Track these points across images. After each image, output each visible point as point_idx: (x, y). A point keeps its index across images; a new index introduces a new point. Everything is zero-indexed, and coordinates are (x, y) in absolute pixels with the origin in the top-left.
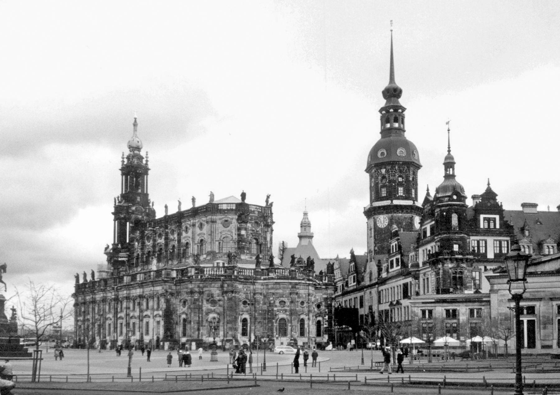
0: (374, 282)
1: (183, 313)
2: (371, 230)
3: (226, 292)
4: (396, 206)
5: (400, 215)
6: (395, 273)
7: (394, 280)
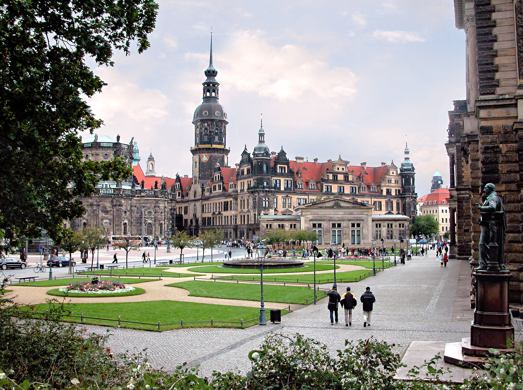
0: (197, 198)
3: (115, 205)
4: (214, 149)
6: (217, 194)
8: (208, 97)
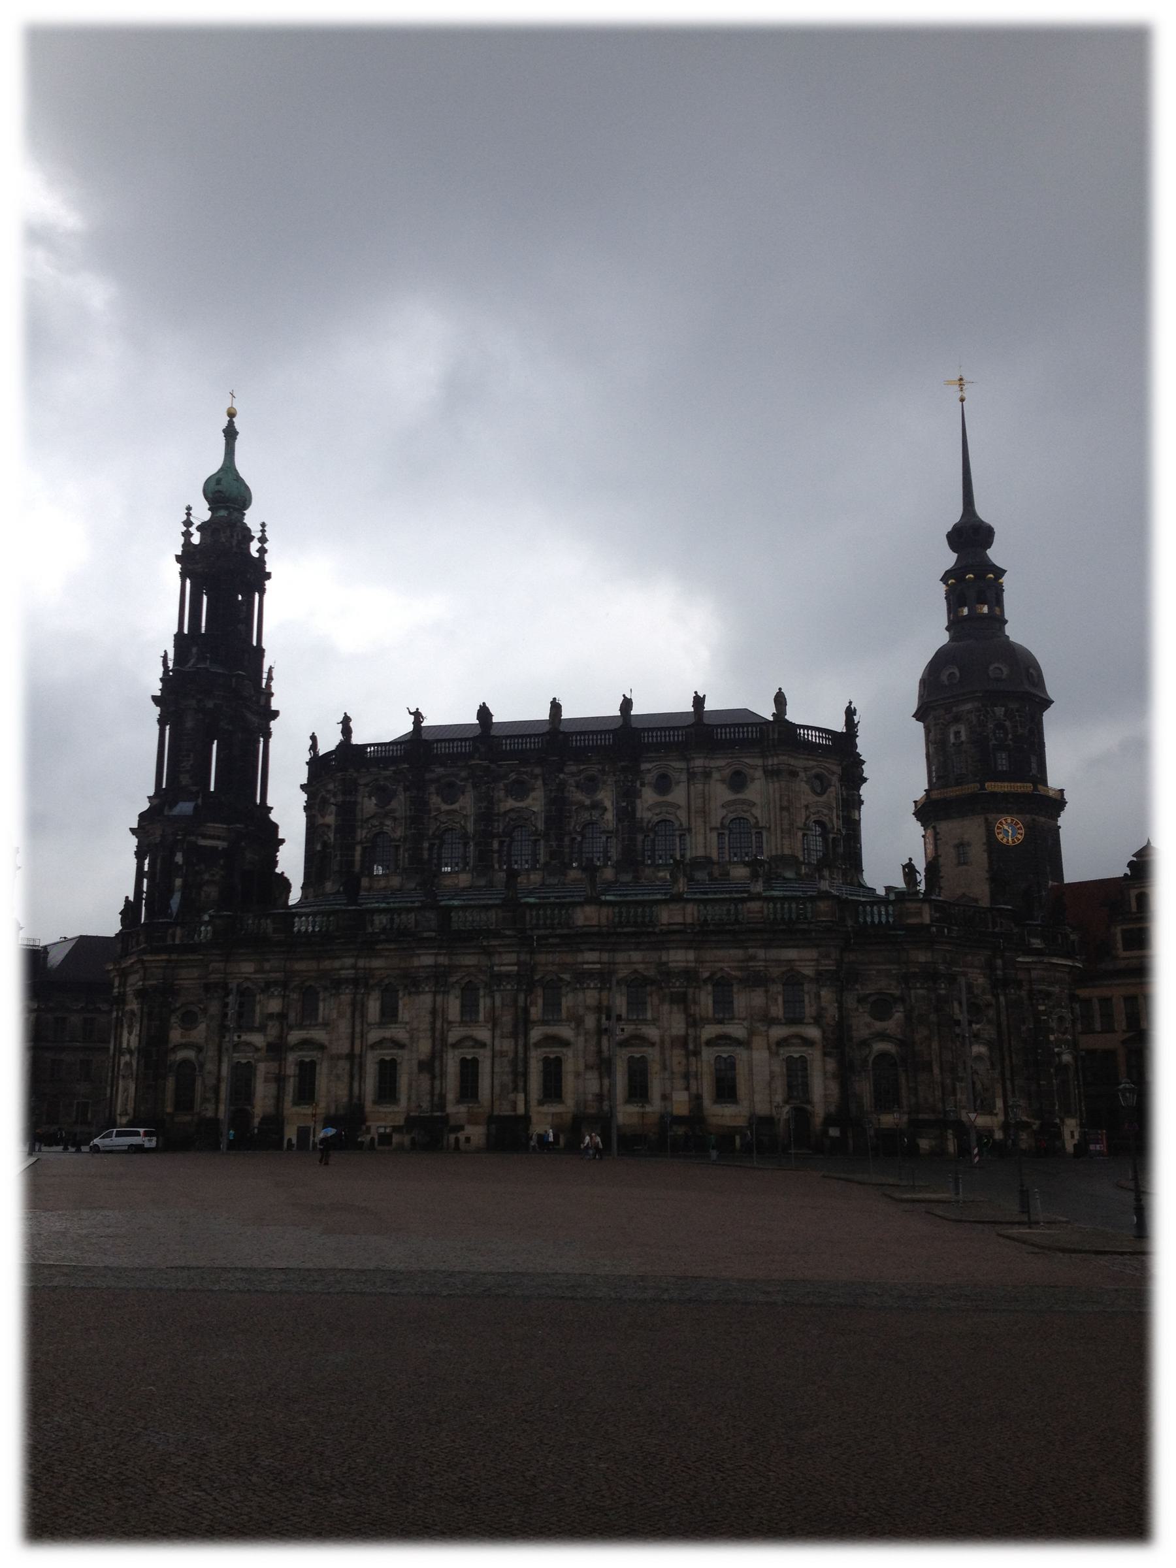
1: (882, 1036)
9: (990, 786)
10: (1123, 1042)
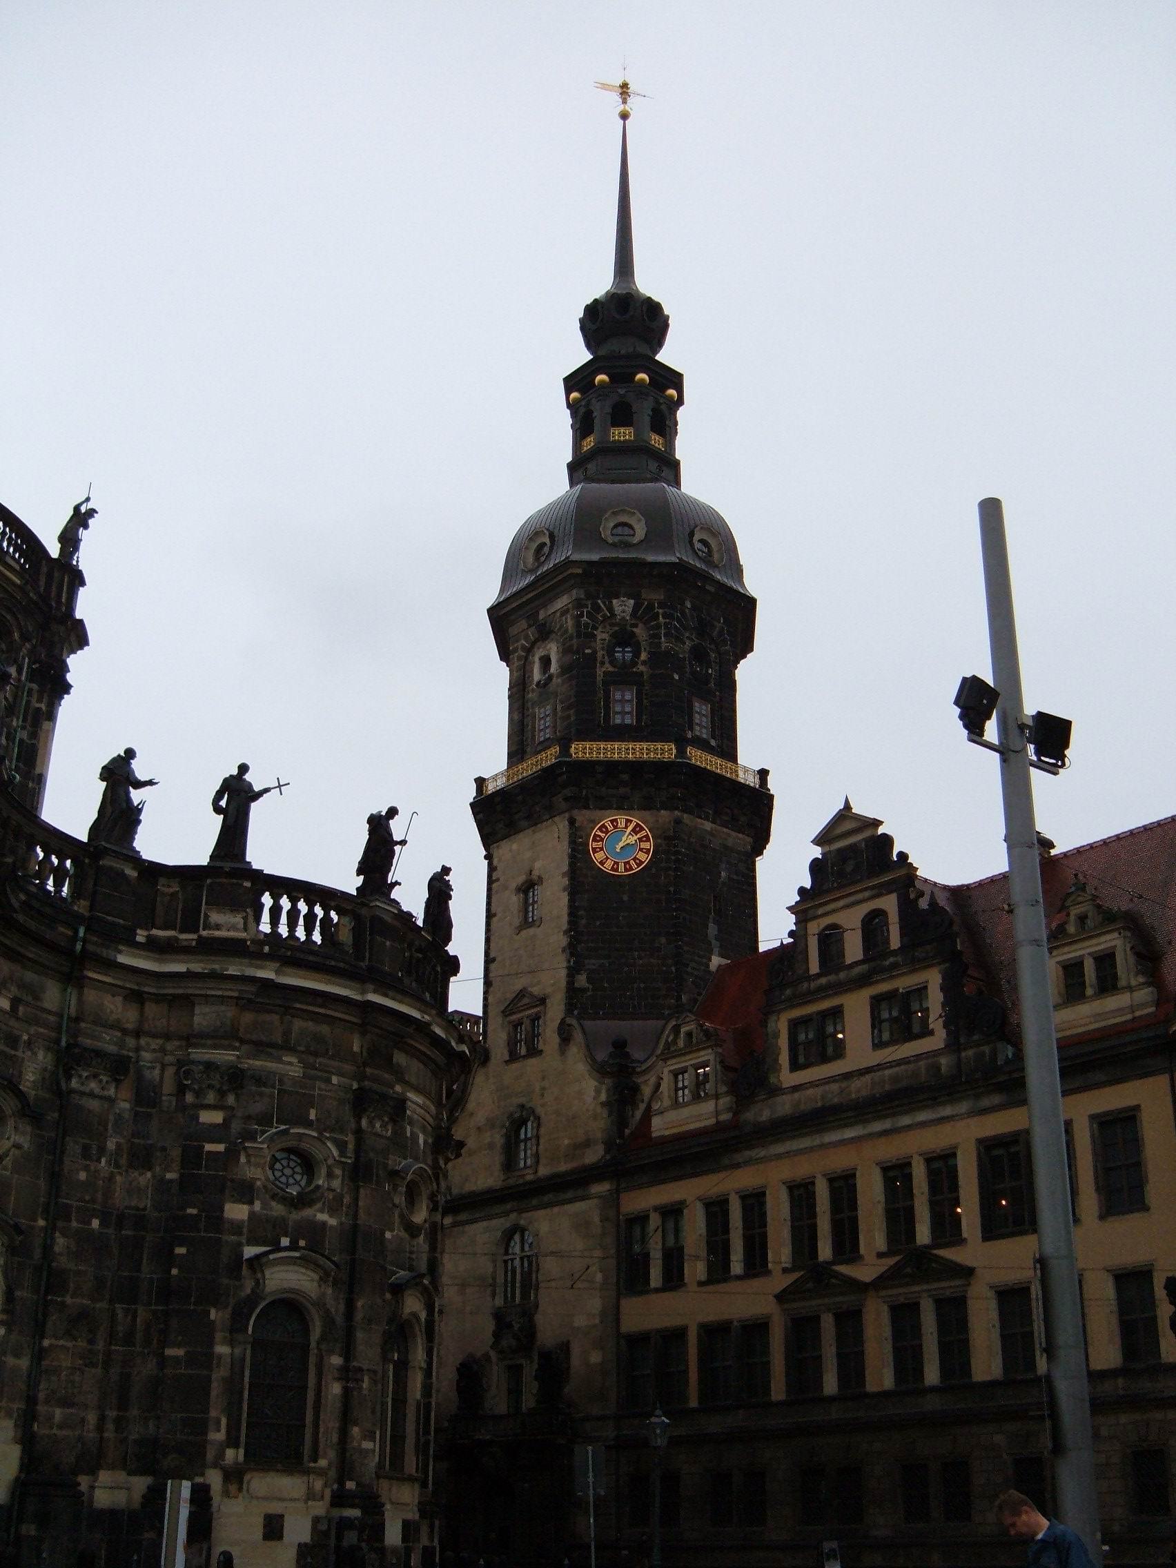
2: (528, 887)
5: (708, 826)
6: (860, 1088)
7: (849, 1133)
8: (623, 449)
9: (582, 750)
10: (781, 1297)
